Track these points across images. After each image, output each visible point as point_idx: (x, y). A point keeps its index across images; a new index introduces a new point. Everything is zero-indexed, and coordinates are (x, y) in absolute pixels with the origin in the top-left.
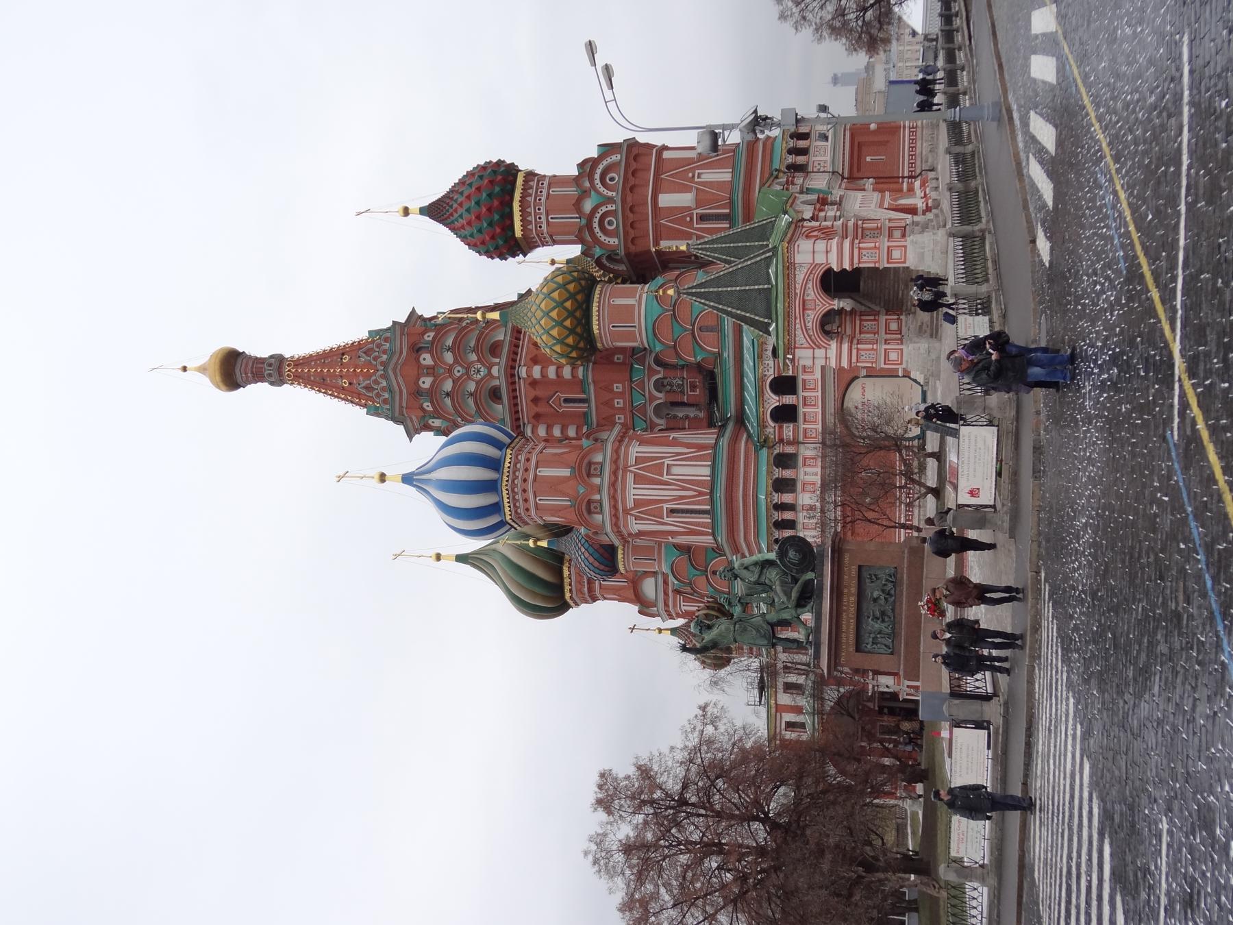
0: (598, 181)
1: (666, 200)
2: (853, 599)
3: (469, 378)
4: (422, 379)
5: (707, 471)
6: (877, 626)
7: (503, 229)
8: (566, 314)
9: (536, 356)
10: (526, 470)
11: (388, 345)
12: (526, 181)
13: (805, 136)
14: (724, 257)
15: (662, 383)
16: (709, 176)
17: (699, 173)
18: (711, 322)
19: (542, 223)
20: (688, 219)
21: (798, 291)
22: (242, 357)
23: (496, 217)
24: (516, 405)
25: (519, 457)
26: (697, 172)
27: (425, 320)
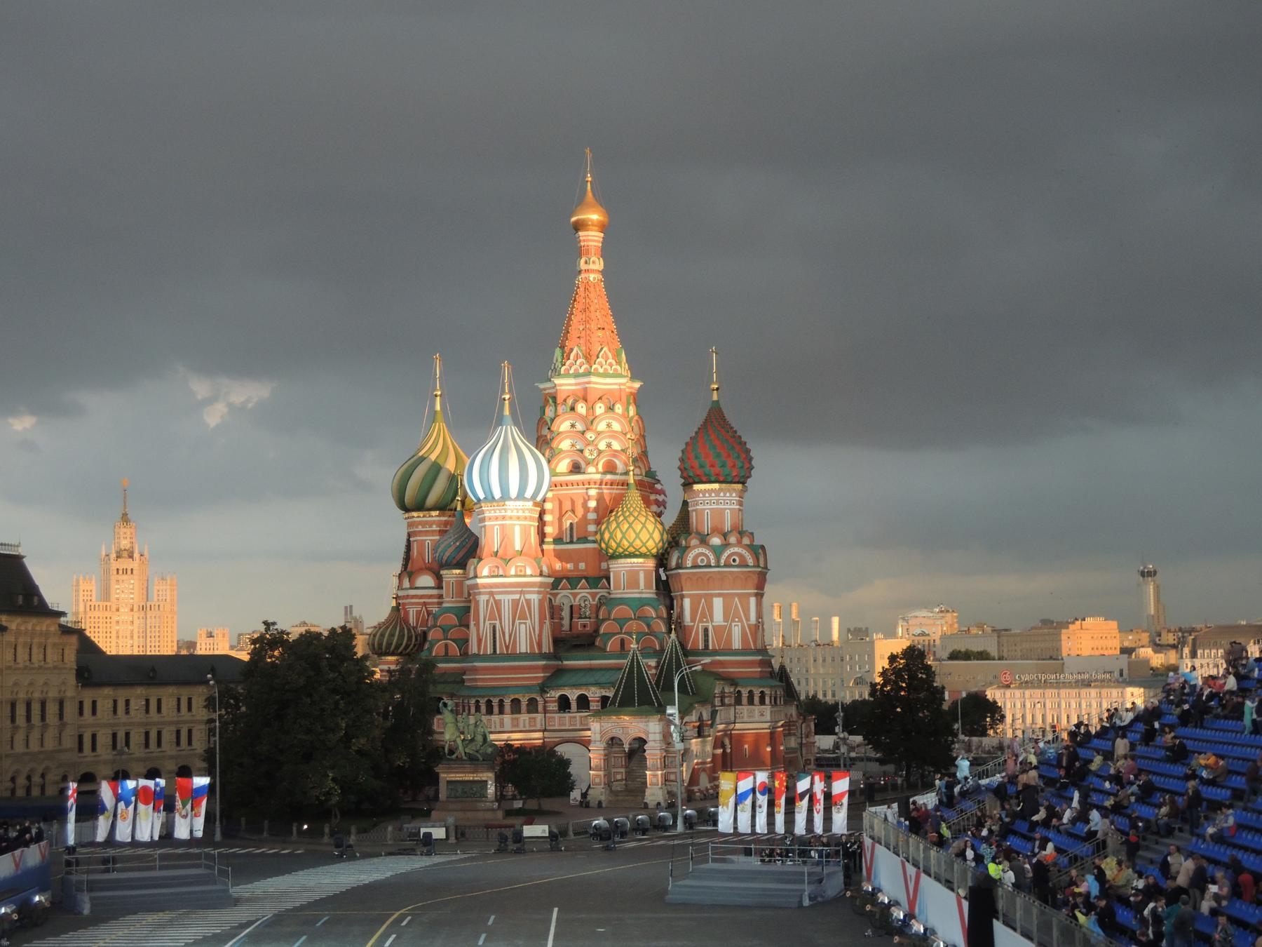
1: (718, 604)
2: (471, 778)
4: (584, 406)
5: (523, 650)
6: (460, 790)
10: (518, 518)
11: (611, 372)
13: (762, 702)
16: (736, 632)
17: (738, 625)
19: (704, 505)
20: (705, 620)
21: (633, 724)
23: (707, 470)
25: (527, 511)
26: (740, 624)
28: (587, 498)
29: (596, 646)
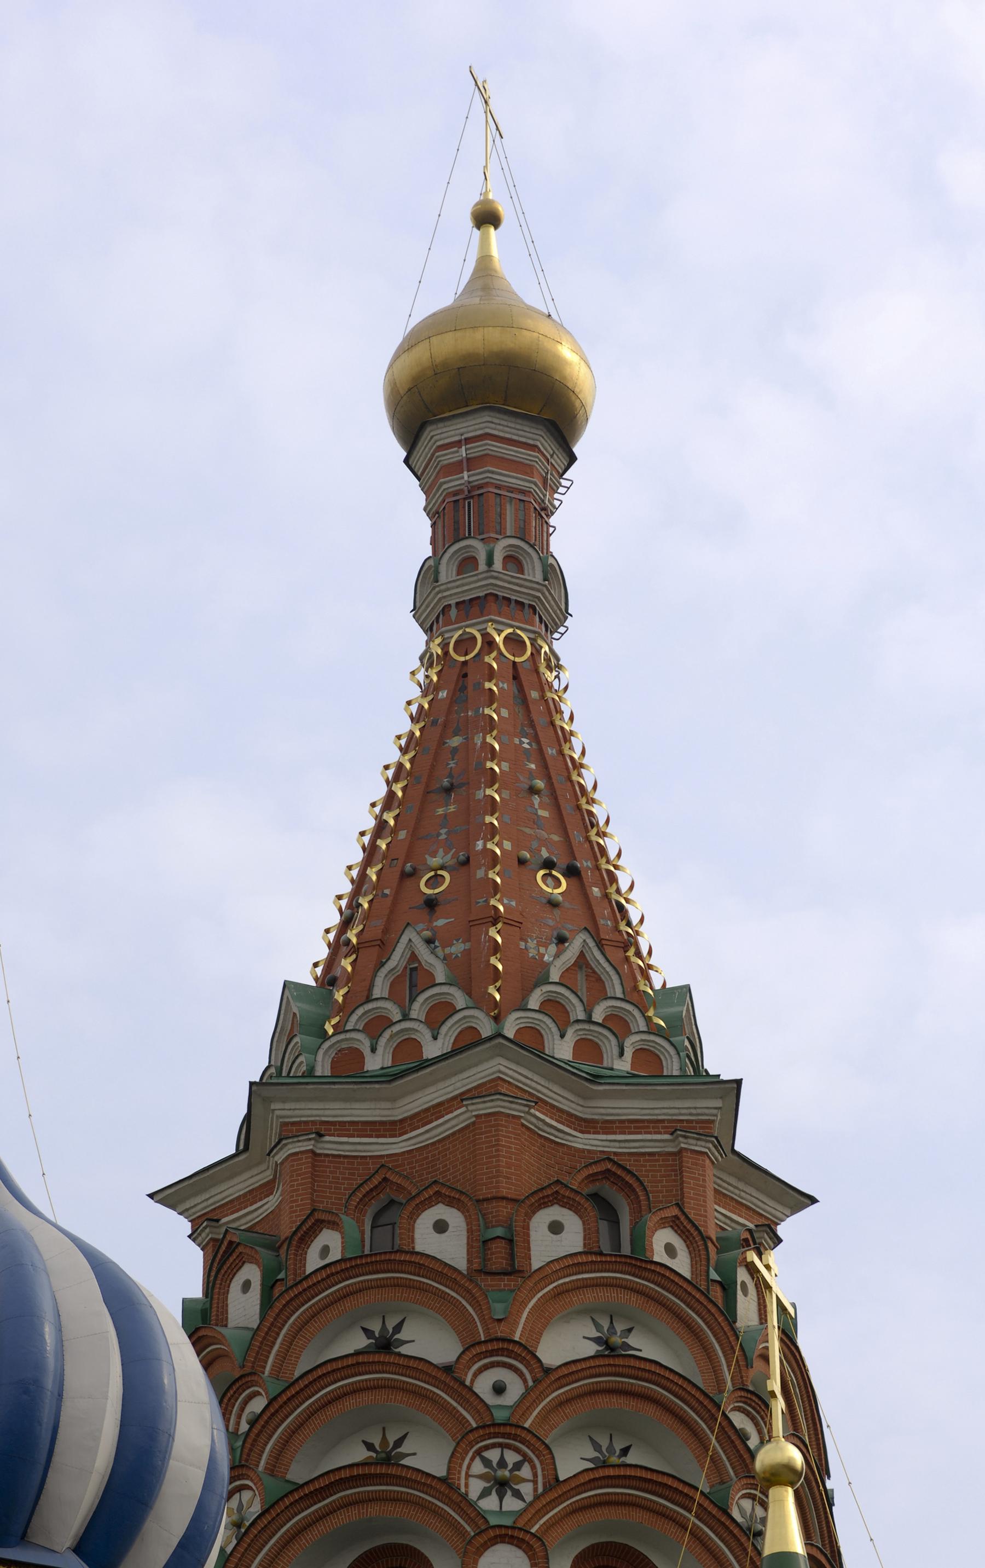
4: (454, 1218)
11: (624, 1065)
22: (547, 444)
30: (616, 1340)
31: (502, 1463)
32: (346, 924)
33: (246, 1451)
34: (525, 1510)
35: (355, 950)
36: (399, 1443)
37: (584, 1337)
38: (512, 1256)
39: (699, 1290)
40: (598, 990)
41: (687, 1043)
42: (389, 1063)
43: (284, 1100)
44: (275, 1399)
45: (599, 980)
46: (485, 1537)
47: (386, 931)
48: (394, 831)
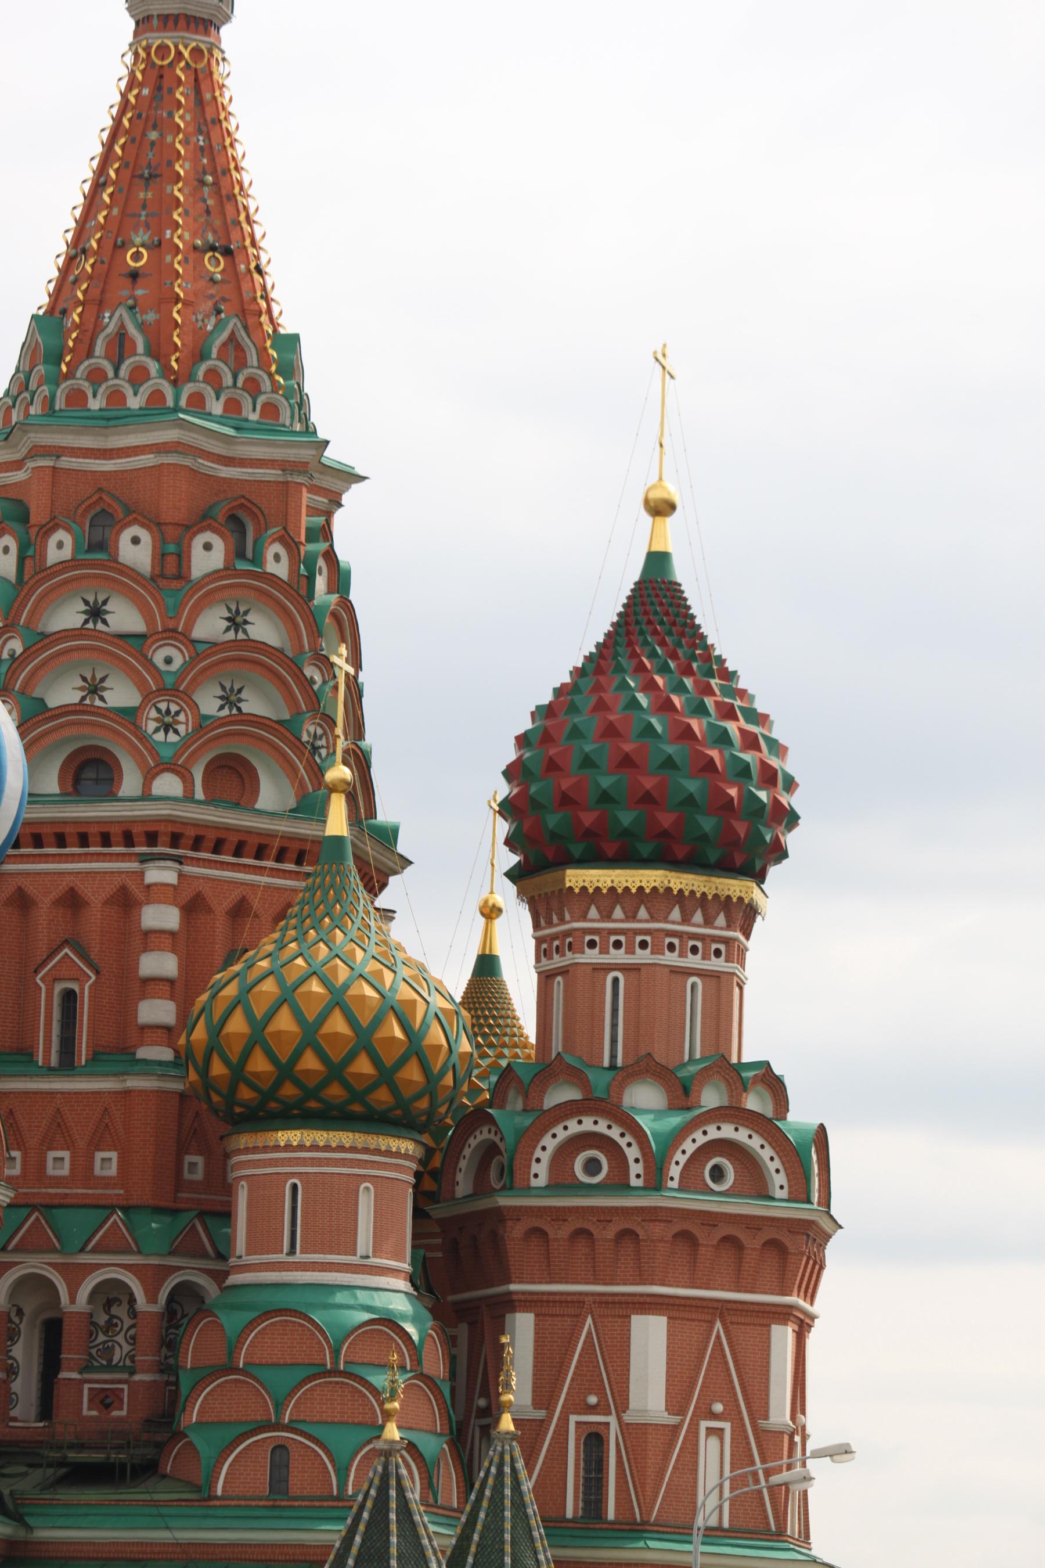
0: (713, 1134)
3: (148, 697)
7: (588, 834)
8: (336, 1056)
9: (210, 910)
11: (254, 417)
12: (727, 904)
14: (476, 1537)
15: (117, 1301)
17: (722, 1430)
18: (299, 1481)
19: (604, 951)
20: (593, 1400)
23: (626, 818)
24: (61, 841)
26: (727, 1426)
27: (325, 533)
28: (141, 896)
29: (164, 1476)
30: (239, 619)
31: (168, 712)
32: (70, 260)
33: (8, 677)
34: (180, 741)
35: (83, 304)
36: (103, 680)
37: (221, 618)
38: (179, 566)
39: (293, 589)
40: (241, 363)
41: (296, 386)
42: (104, 405)
43: (36, 432)
44: (28, 648)
45: (243, 350)
46: (158, 769)
47: (103, 292)
48: (109, 207)
